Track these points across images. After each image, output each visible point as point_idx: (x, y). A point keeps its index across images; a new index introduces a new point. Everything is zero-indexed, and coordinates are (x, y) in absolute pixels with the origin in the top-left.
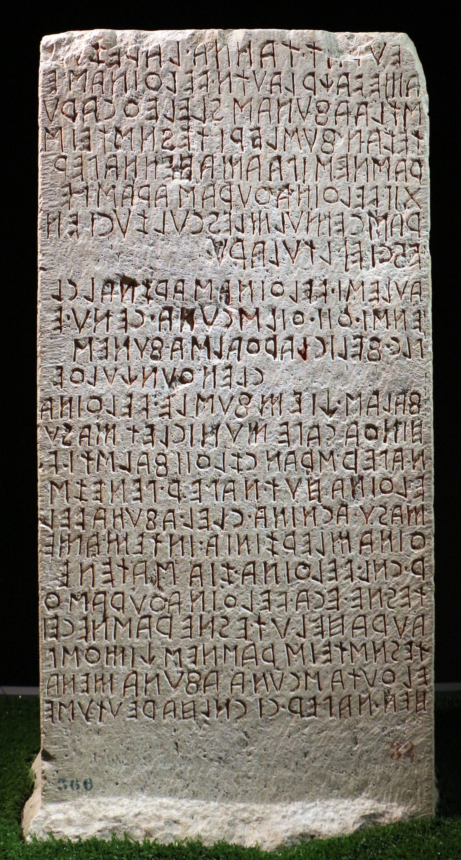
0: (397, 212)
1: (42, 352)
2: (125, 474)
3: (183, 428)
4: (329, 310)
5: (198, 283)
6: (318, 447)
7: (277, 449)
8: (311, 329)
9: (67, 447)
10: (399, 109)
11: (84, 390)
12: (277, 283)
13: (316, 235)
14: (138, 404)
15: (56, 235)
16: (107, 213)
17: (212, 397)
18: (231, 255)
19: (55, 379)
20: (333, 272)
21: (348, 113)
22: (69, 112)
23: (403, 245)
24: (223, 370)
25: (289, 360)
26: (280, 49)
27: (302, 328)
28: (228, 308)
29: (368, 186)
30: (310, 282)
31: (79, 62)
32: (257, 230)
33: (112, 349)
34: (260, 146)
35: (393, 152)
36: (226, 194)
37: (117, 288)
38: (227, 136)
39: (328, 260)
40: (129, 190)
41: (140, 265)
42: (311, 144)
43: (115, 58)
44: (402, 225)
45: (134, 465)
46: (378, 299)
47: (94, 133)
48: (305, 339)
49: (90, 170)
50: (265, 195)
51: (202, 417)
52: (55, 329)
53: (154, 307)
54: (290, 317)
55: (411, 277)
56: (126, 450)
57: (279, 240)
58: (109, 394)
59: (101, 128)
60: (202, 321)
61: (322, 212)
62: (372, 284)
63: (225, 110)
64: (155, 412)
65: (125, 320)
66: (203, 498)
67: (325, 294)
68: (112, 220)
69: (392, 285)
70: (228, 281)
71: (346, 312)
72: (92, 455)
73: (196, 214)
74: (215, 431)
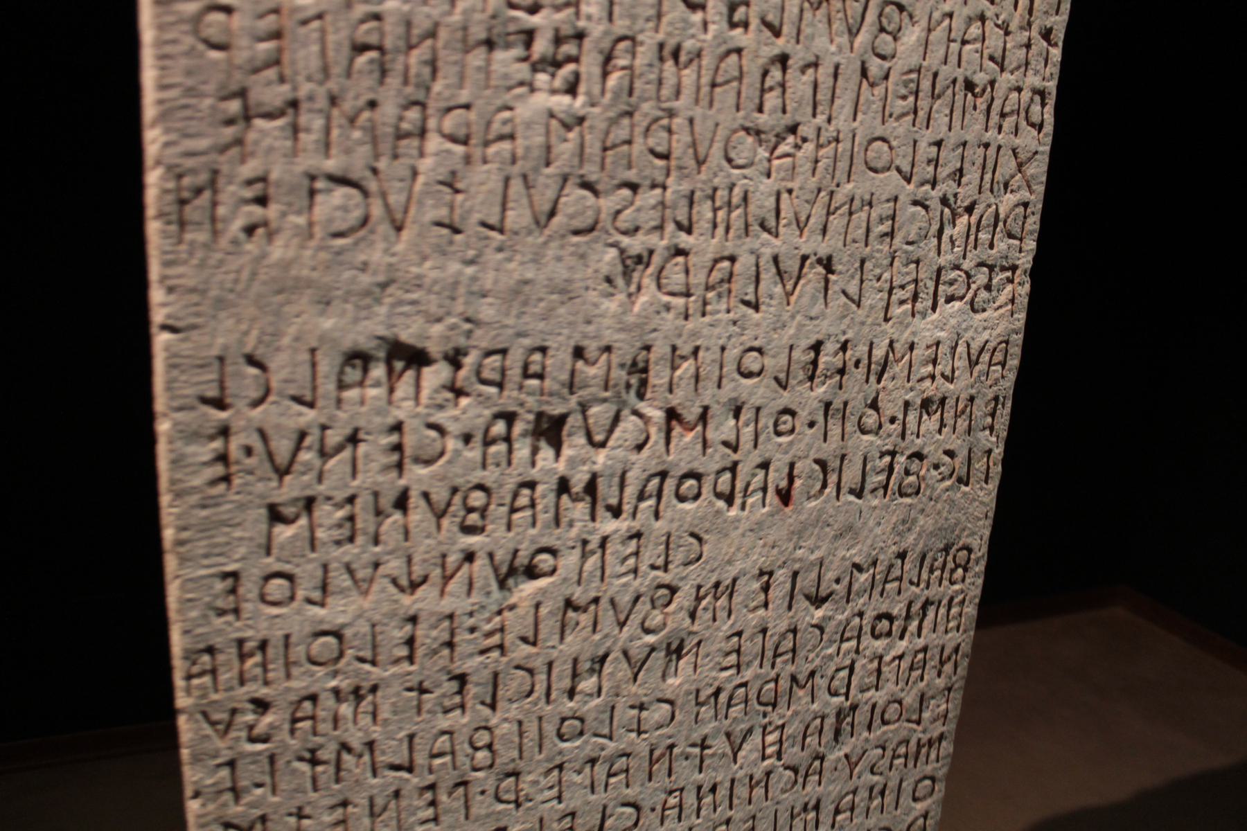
0: (993, 200)
1: (180, 543)
2: (401, 779)
3: (531, 672)
4: (846, 404)
5: (579, 353)
6: (791, 668)
7: (716, 684)
8: (805, 445)
9: (260, 747)
11: (298, 619)
12: (751, 349)
13: (840, 244)
14: (428, 635)
15: (202, 236)
16: (354, 176)
17: (596, 600)
18: (659, 287)
19: (220, 603)
20: (863, 323)
23: (991, 268)
24: (623, 543)
25: (759, 508)
27: (791, 443)
28: (643, 407)
29: (952, 139)
30: (817, 347)
32: (720, 230)
33: (365, 521)
34: (746, 25)
35: (1002, 70)
36: (658, 140)
37: (378, 371)
39: (856, 298)
40: (413, 114)
41: (441, 312)
42: (853, 33)
44: (995, 226)
45: (420, 759)
46: (933, 377)
48: (792, 466)
49: (305, 56)
50: (746, 146)
51: (573, 643)
52: (214, 482)
53: (468, 413)
54: (766, 421)
55: (995, 333)
56: (402, 734)
57: (767, 252)
58: (362, 621)
60: (582, 440)
61: (858, 192)
62: (928, 347)
64: (471, 648)
65: (398, 448)
66: (566, 795)
67: (842, 372)
68: (366, 193)
69: (961, 349)
70: (648, 348)
71: (874, 405)
72: (323, 755)
73: (587, 185)
74: (597, 666)
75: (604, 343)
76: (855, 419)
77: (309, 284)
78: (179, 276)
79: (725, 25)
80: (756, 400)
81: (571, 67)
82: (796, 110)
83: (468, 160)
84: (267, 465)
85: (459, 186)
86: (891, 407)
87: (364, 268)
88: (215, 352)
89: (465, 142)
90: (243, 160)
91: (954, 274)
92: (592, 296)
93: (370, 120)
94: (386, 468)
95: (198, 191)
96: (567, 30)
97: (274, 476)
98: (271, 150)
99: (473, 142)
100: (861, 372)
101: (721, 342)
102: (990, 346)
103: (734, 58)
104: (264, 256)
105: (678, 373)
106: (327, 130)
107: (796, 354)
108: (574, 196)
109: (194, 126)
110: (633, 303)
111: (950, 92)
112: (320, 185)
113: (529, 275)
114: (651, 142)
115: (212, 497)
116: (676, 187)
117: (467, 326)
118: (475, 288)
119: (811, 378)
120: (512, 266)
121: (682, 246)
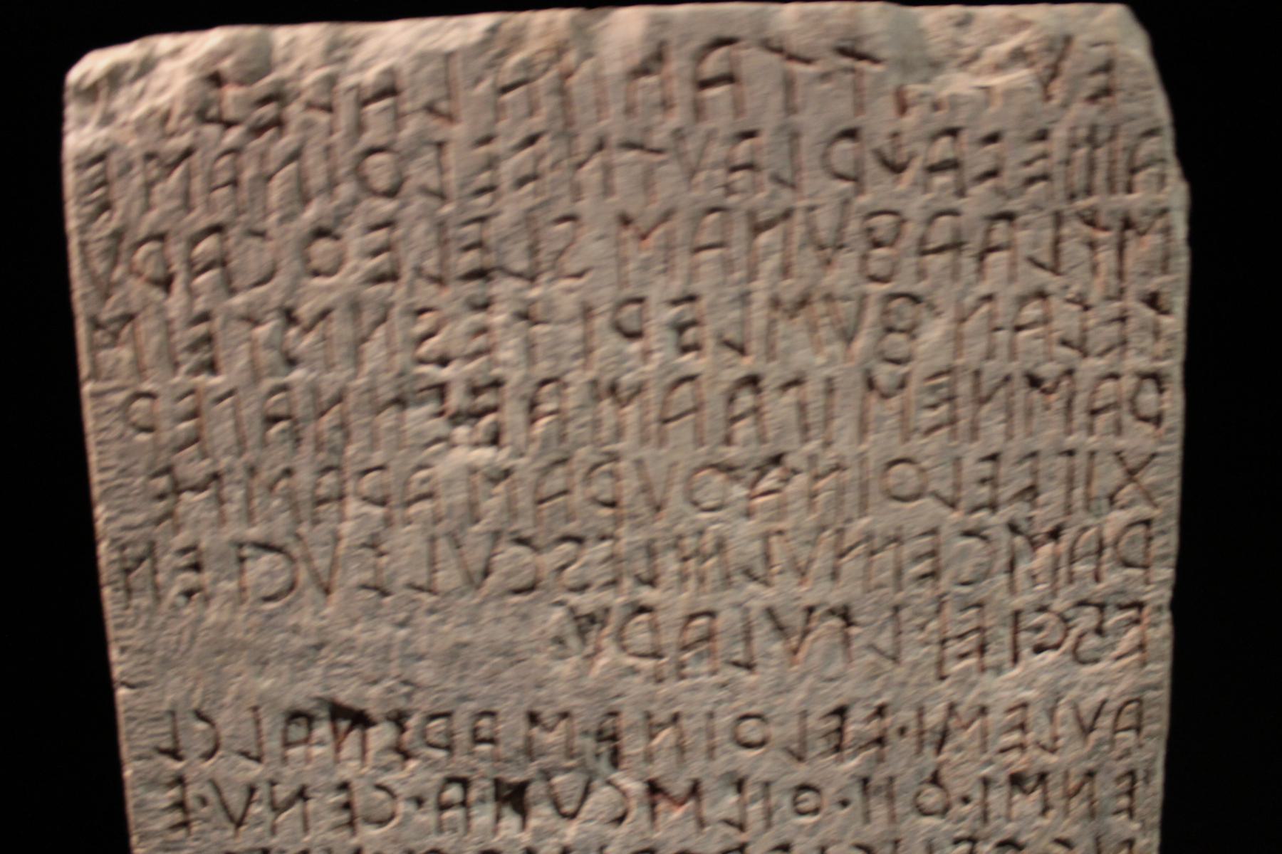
4: (891, 779)
5: (533, 718)
10: (1106, 229)
12: (747, 717)
16: (278, 542)
20: (903, 684)
21: (956, 245)
22: (151, 270)
23: (1101, 607)
26: (753, 60)
27: (816, 825)
29: (1013, 450)
30: (841, 712)
31: (172, 125)
32: (692, 583)
36: (603, 487)
37: (323, 730)
38: (600, 322)
40: (329, 479)
41: (377, 675)
42: (848, 337)
43: (269, 111)
47: (224, 325)
49: (221, 432)
52: (175, 827)
57: (757, 605)
59: (242, 311)
63: (592, 246)
65: (347, 806)
67: (880, 741)
68: (292, 559)
69: (1062, 711)
71: (935, 780)
73: (522, 541)
75: (561, 707)
76: (908, 797)
77: (245, 646)
78: (130, 638)
79: (670, 351)
80: (761, 774)
81: (489, 419)
82: (778, 437)
83: (388, 521)
84: (221, 816)
85: (384, 547)
86: (957, 789)
87: (296, 630)
88: (165, 707)
89: (383, 503)
90: (177, 529)
91: (1040, 618)
92: (541, 659)
93: (287, 487)
94: (336, 827)
95: (140, 560)
96: (481, 381)
97: (231, 827)
98: (197, 522)
99: (393, 503)
100: (908, 743)
101: (708, 708)
102: (1113, 706)
103: (685, 388)
104: (200, 620)
105: (656, 741)
106: (248, 498)
107: (811, 722)
108: (509, 553)
109: (130, 503)
110: (592, 665)
111: (1001, 393)
112: (247, 551)
113: (466, 637)
114: (594, 489)
115: (175, 842)
116: (628, 538)
117: (406, 689)
118: (410, 650)
119: (838, 748)
120: (446, 628)
121: (643, 603)
